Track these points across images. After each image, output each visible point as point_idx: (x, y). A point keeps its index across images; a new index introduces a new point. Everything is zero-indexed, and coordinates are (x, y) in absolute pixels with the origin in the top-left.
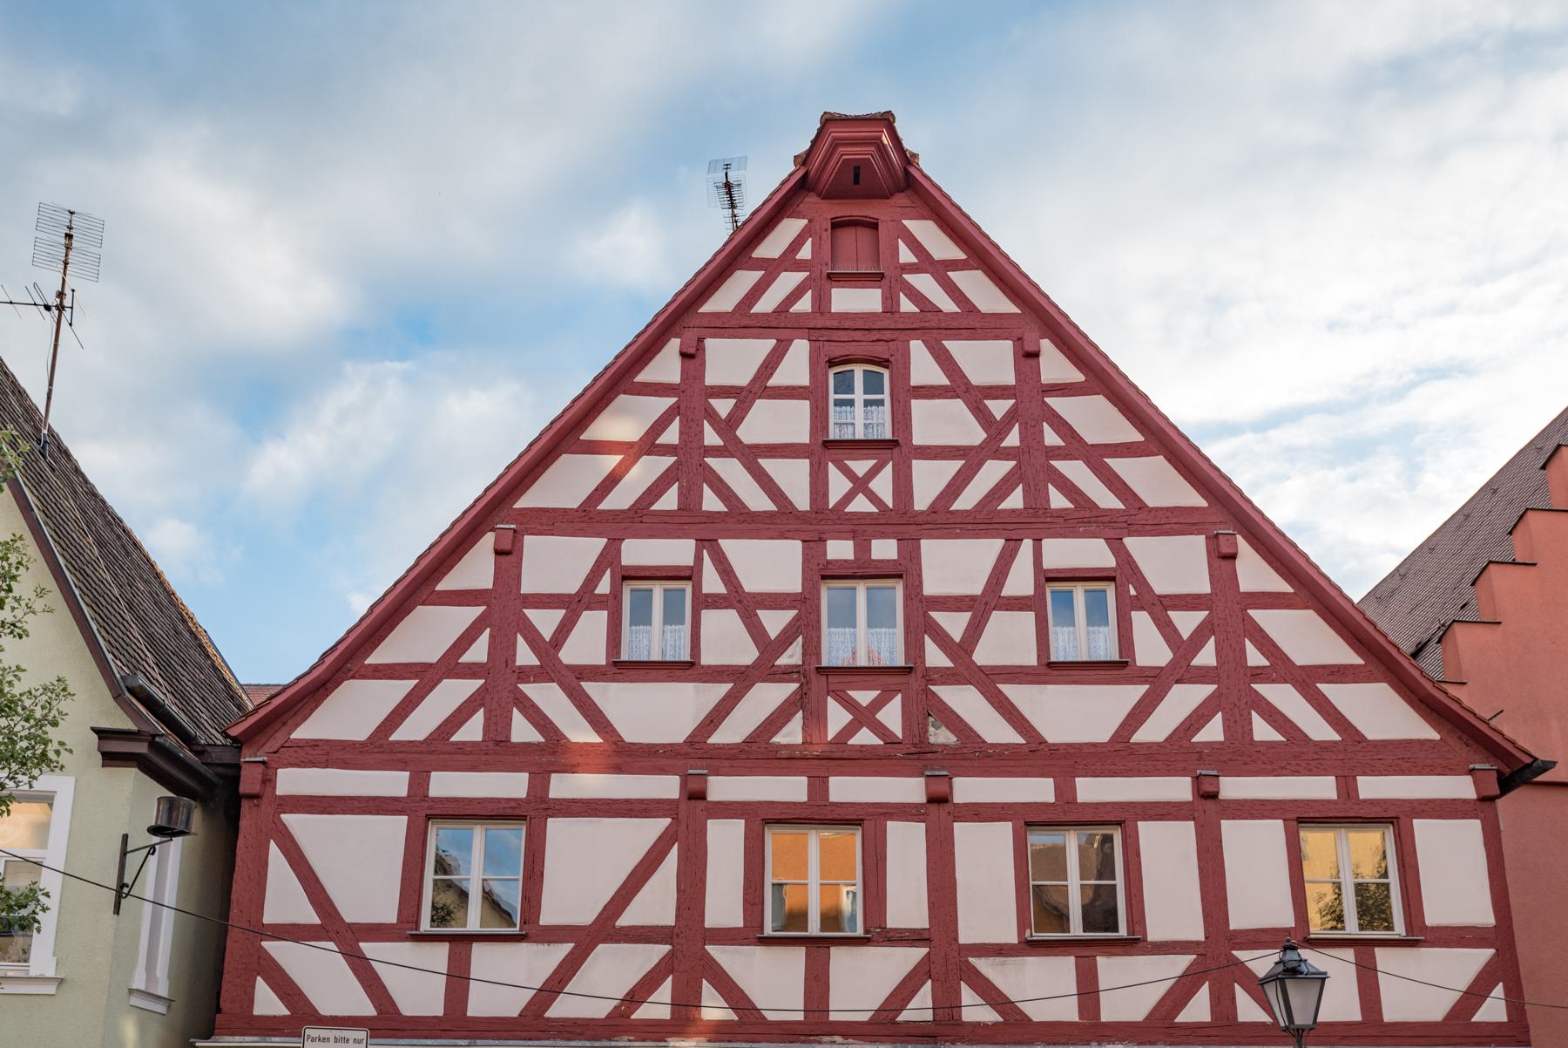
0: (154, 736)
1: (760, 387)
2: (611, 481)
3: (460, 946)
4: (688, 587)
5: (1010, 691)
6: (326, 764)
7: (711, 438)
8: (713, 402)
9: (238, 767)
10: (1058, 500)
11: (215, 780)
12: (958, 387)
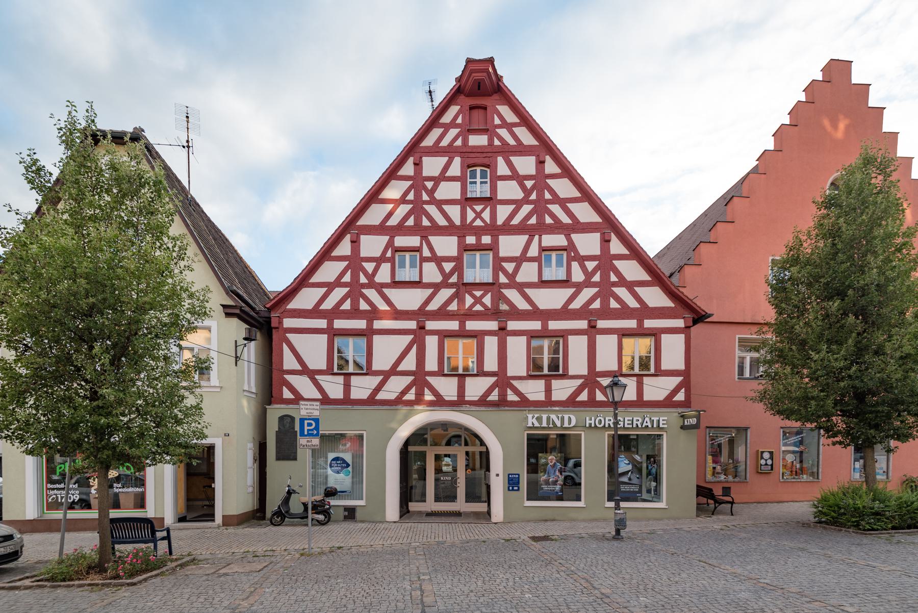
0: (241, 307)
1: (442, 177)
2: (390, 215)
3: (347, 377)
4: (418, 254)
6: (299, 317)
7: (425, 197)
8: (426, 183)
9: (270, 318)
10: (548, 220)
11: (263, 322)
12: (515, 176)
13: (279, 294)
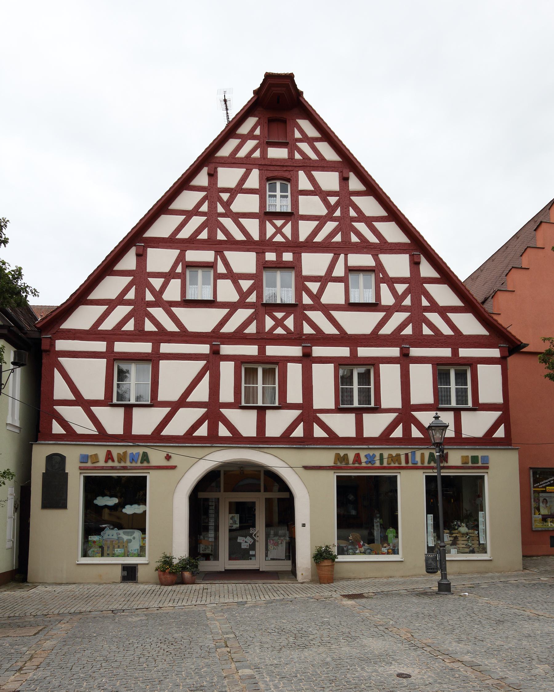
1: (239, 189)
5: (334, 313)
7: (220, 209)
8: (221, 194)
10: (354, 239)
12: (317, 191)
13: (52, 312)
